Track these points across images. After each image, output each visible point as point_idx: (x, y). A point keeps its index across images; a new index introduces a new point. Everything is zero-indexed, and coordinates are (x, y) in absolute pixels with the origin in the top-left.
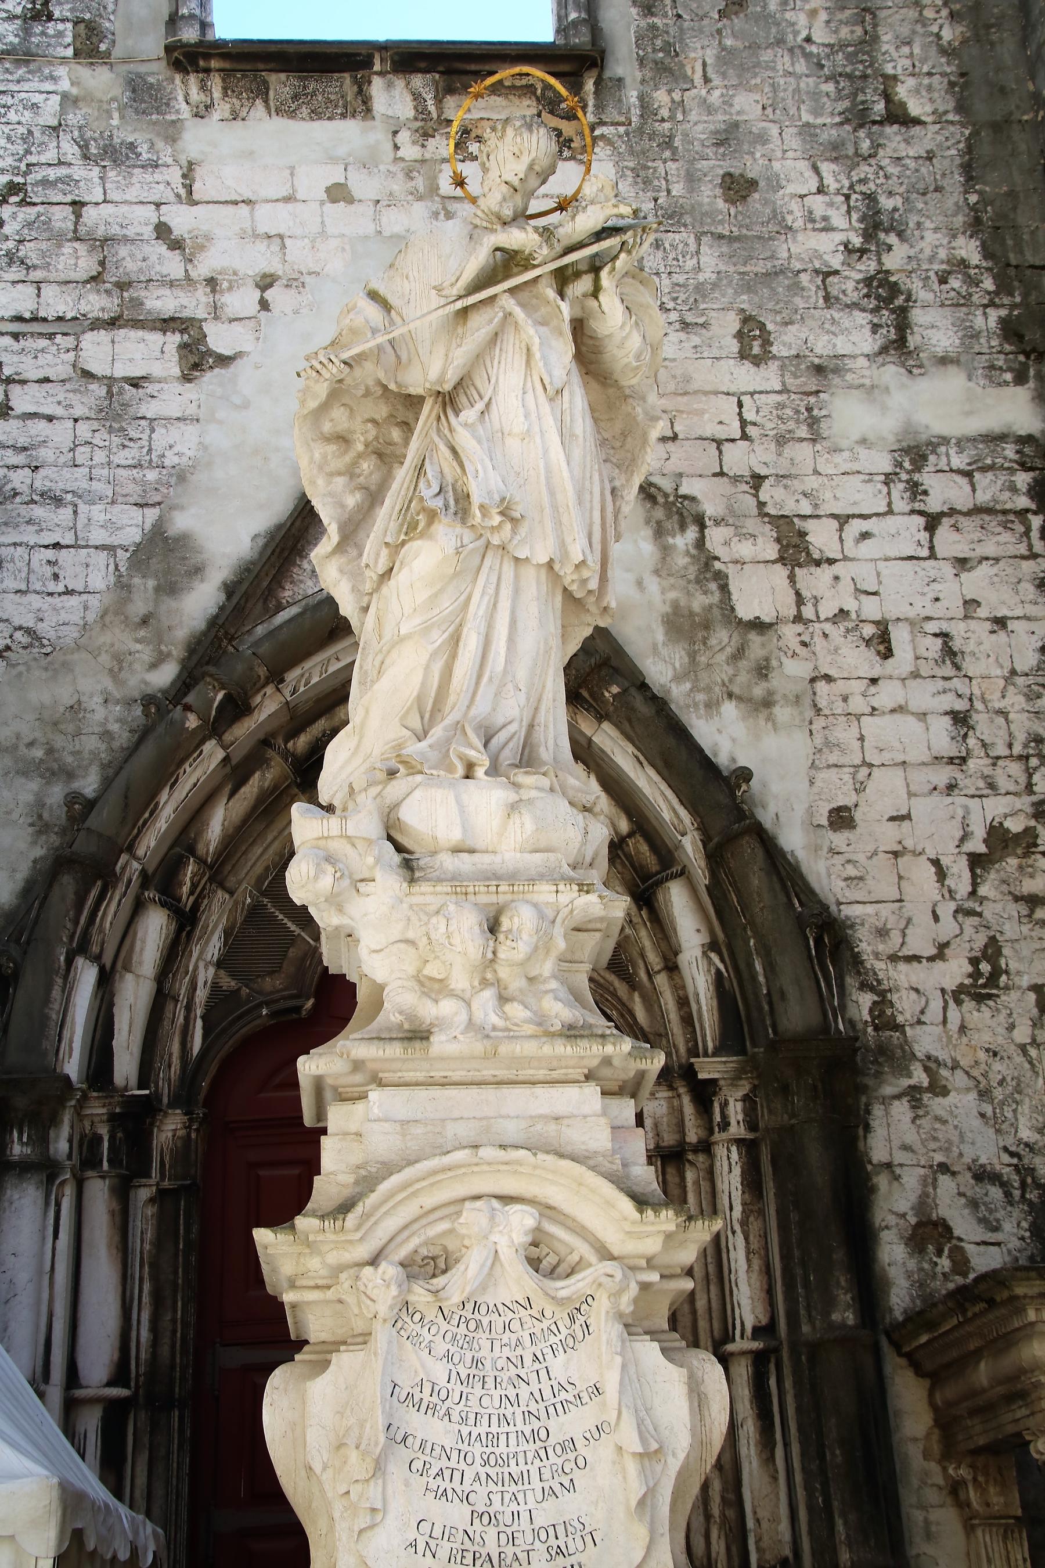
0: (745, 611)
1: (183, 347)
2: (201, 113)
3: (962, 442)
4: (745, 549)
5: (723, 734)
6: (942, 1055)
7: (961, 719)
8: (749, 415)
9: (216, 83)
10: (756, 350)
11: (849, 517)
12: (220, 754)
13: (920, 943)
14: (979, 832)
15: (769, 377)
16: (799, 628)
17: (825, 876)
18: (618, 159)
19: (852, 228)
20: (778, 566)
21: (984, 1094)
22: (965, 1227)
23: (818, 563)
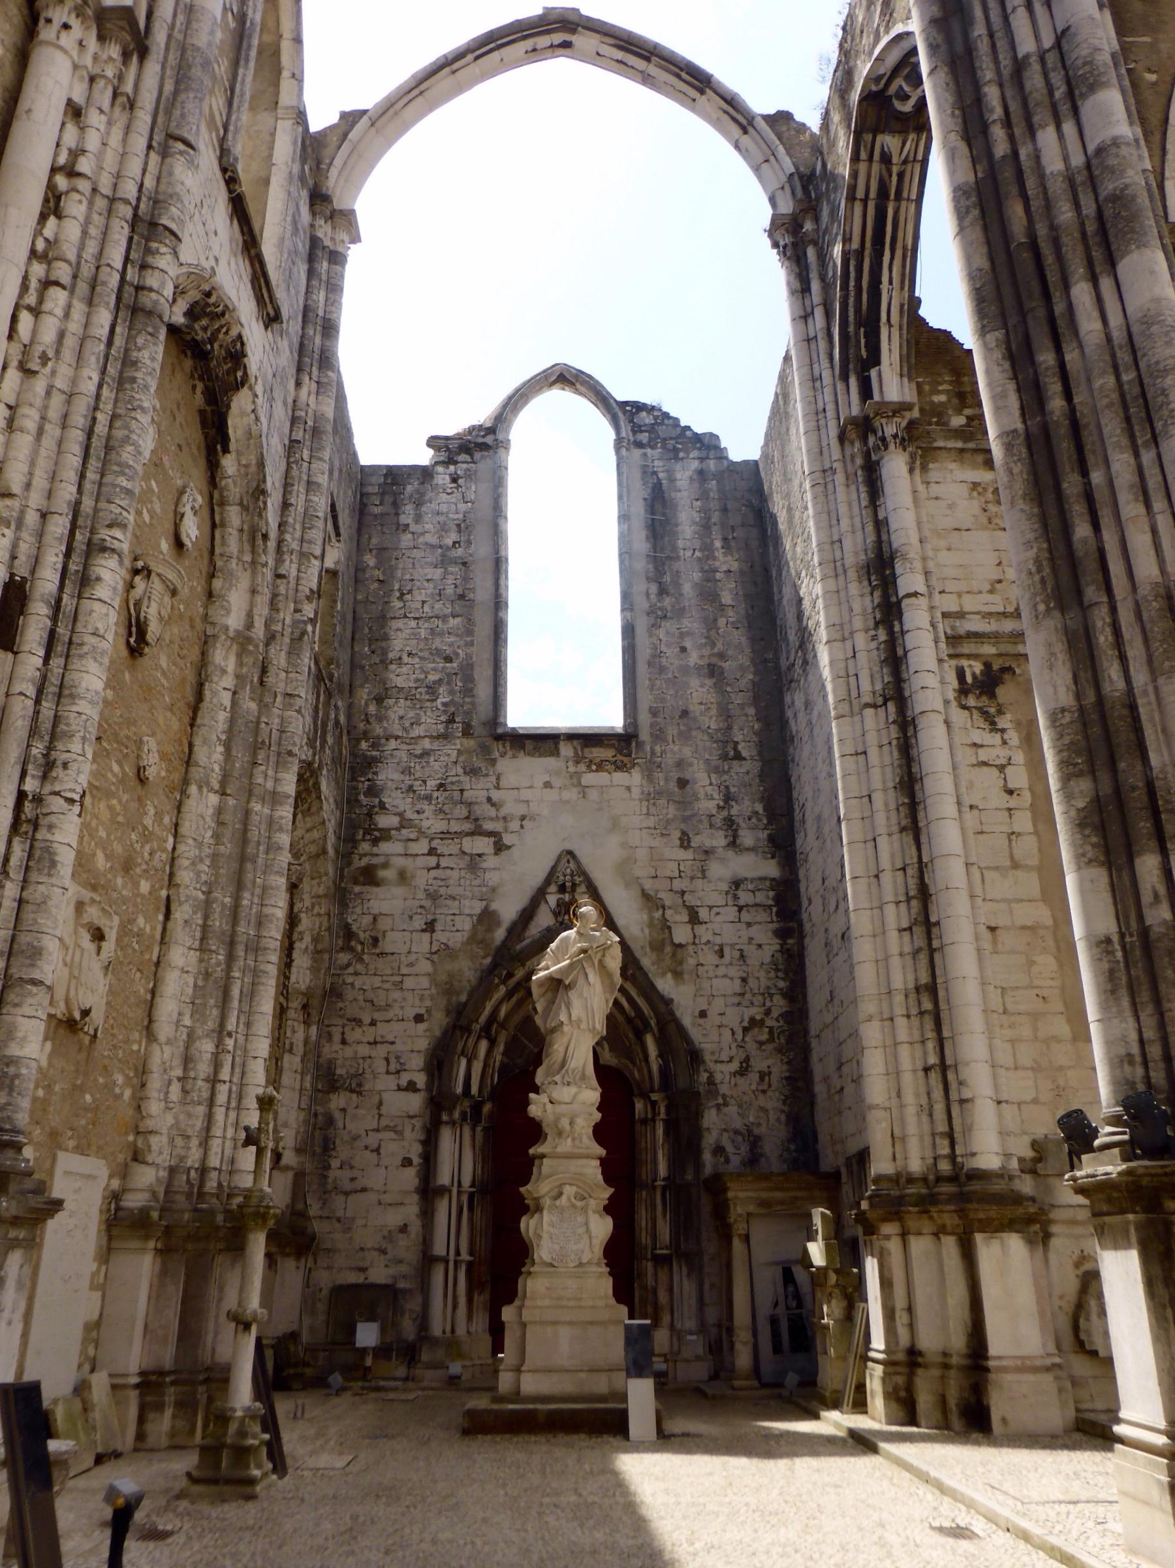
0: (676, 941)
1: (495, 843)
2: (503, 755)
3: (752, 880)
4: (678, 918)
5: (665, 985)
6: (728, 1093)
7: (744, 980)
9: (508, 745)
13: (724, 1057)
14: (747, 1019)
15: (689, 855)
17: (695, 1034)
21: (740, 1106)
22: (730, 1149)
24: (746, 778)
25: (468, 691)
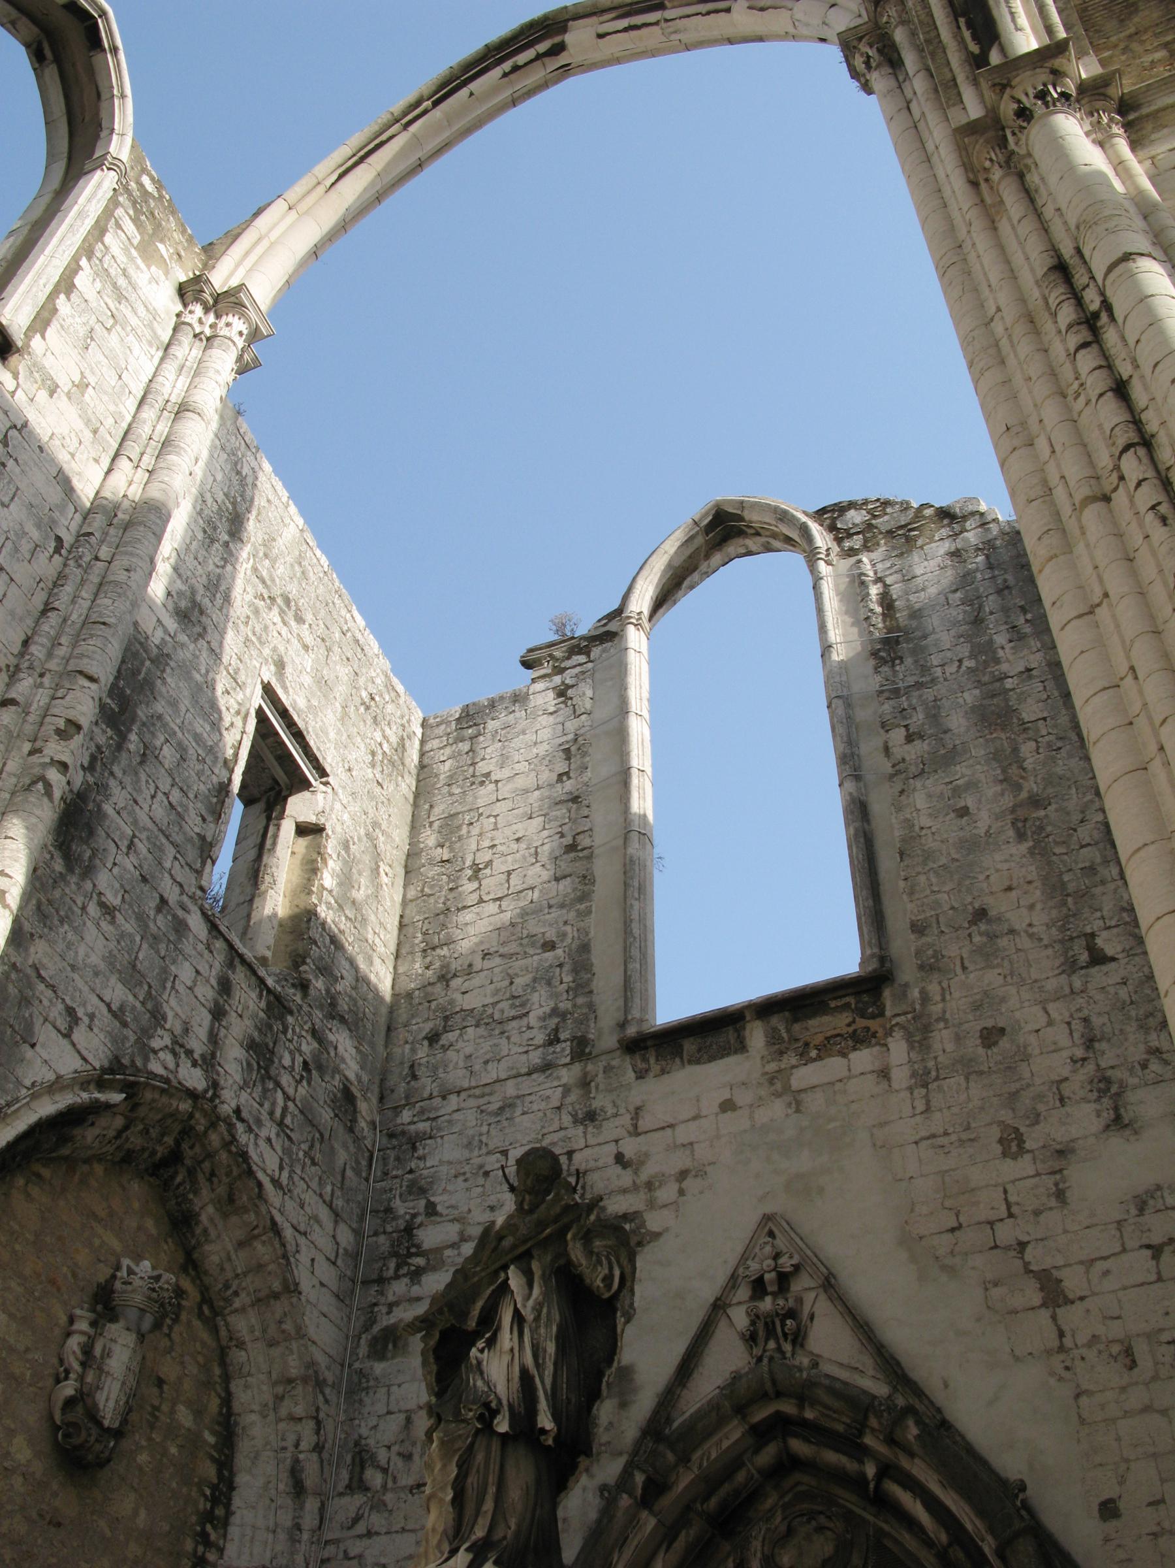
8: (1012, 1199)
10: (1014, 1148)
11: (1093, 1261)
12: (652, 1522)
15: (1024, 1166)
16: (1062, 1357)
18: (909, 1037)
19: (1074, 1044)
20: (1043, 1311)
23: (1072, 1302)
24: (1123, 993)
25: (582, 986)
